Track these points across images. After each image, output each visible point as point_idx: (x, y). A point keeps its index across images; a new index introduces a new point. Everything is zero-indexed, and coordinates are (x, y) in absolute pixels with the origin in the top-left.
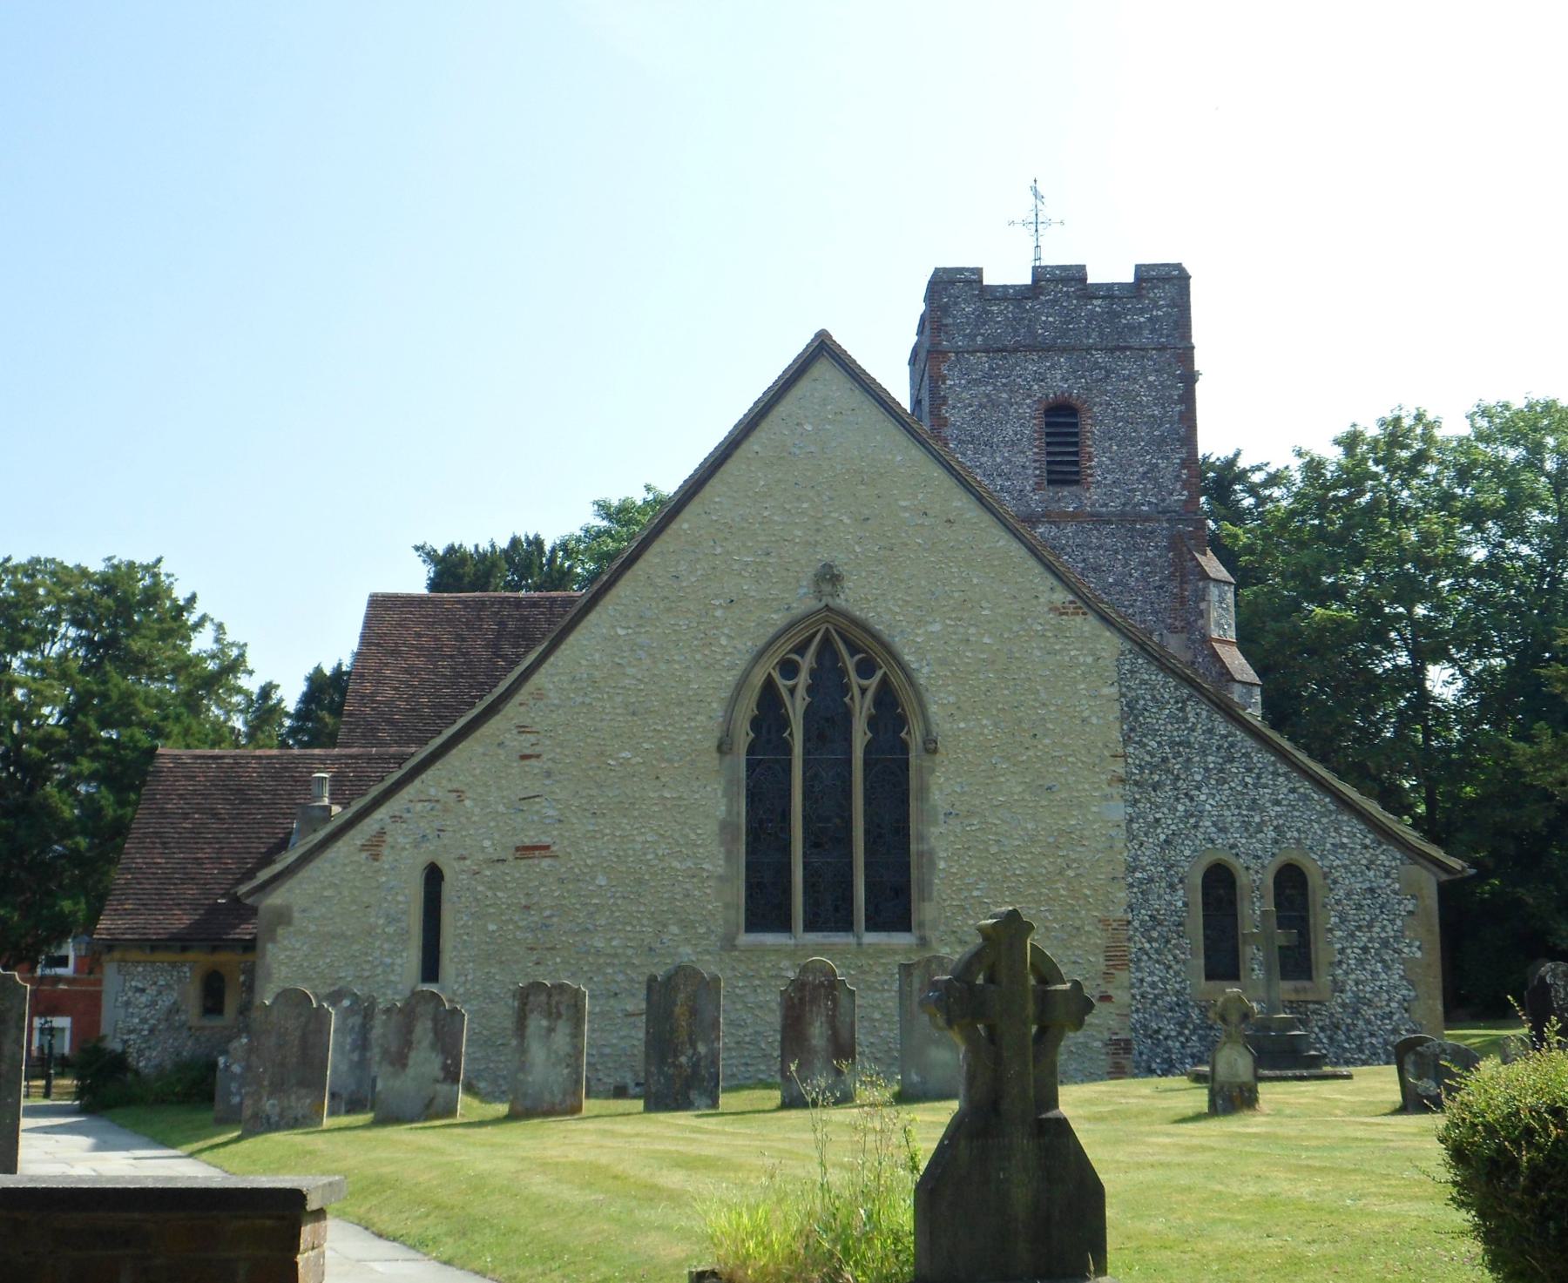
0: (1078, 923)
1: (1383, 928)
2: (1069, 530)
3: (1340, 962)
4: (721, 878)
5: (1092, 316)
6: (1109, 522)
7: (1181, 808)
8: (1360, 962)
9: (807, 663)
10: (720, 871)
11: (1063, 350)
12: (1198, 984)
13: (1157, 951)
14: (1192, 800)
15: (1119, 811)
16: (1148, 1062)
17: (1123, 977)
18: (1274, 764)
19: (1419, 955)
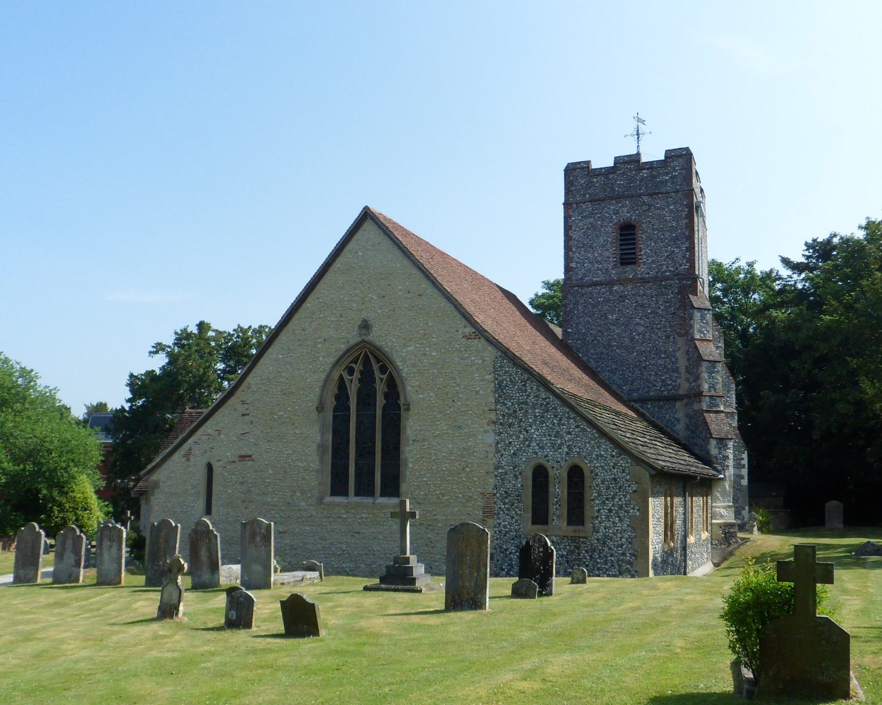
0: (471, 494)
1: (620, 499)
2: (629, 287)
3: (597, 517)
4: (317, 471)
5: (642, 179)
6: (649, 282)
7: (522, 436)
8: (608, 517)
9: (358, 367)
10: (317, 467)
11: (627, 197)
12: (528, 528)
13: (508, 509)
14: (527, 432)
15: (491, 438)
16: (501, 565)
17: (490, 521)
18: (568, 413)
19: (638, 514)
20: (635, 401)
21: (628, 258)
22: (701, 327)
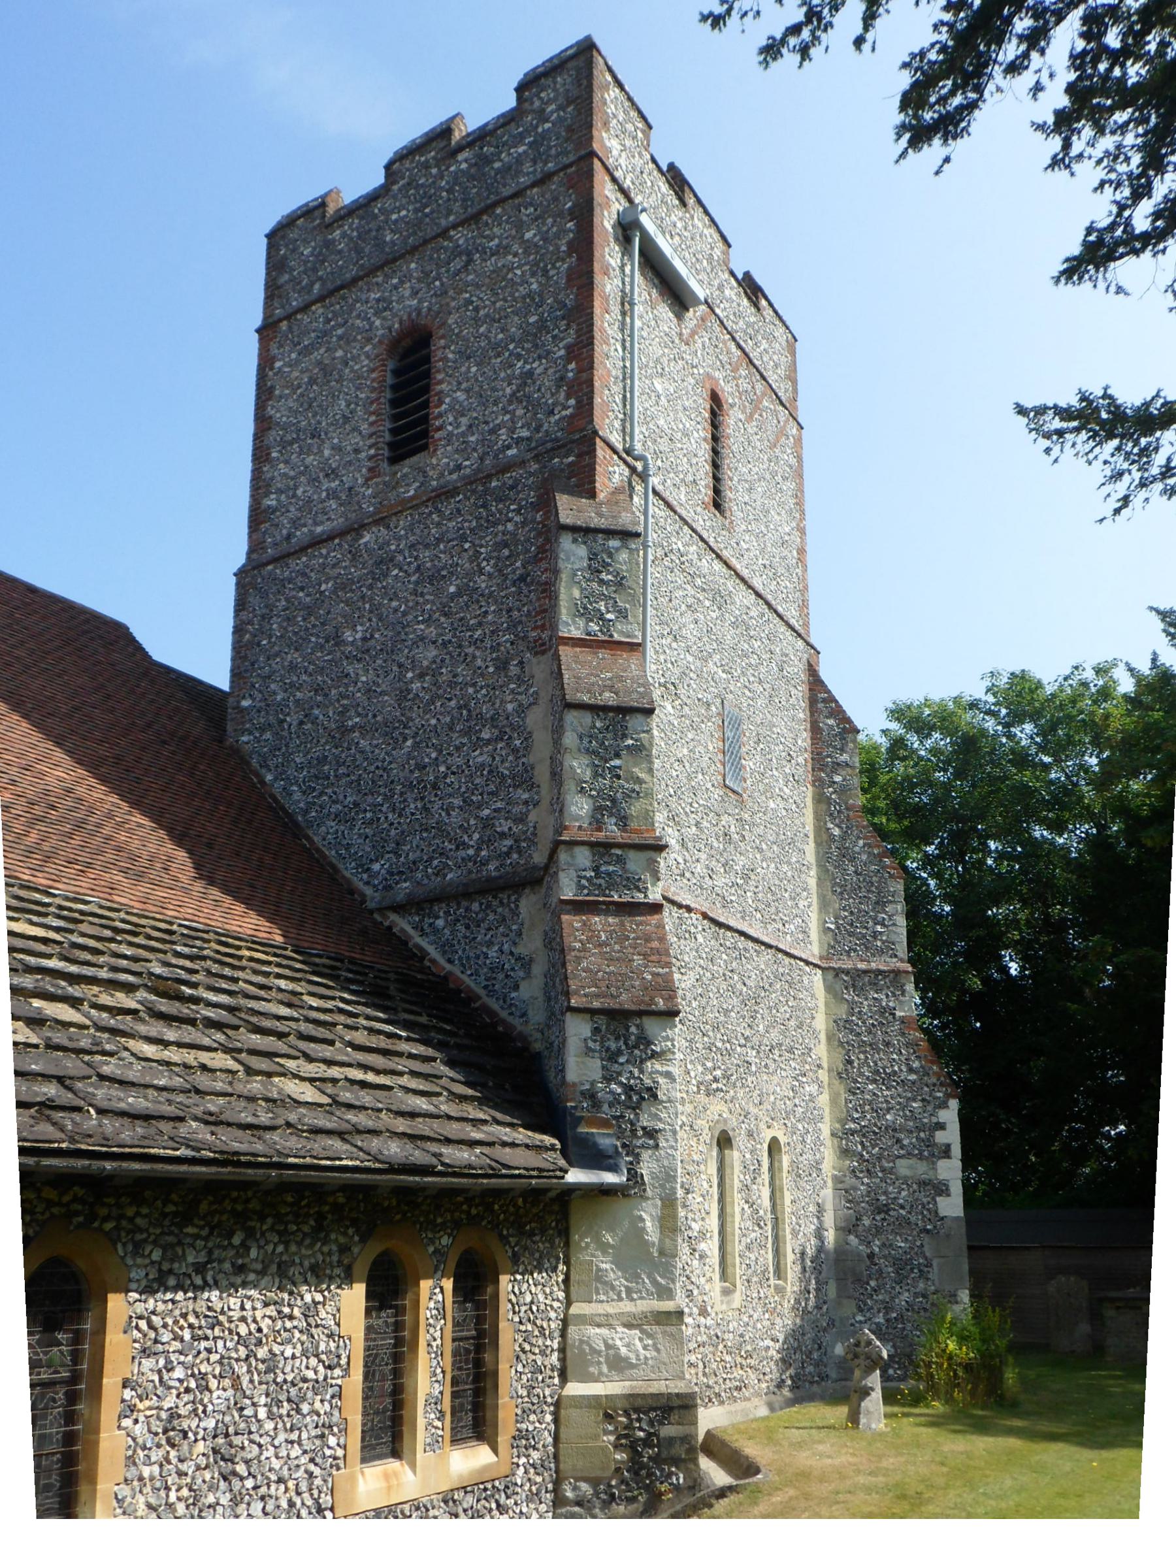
20: (399, 908)
21: (409, 433)
22: (588, 596)
